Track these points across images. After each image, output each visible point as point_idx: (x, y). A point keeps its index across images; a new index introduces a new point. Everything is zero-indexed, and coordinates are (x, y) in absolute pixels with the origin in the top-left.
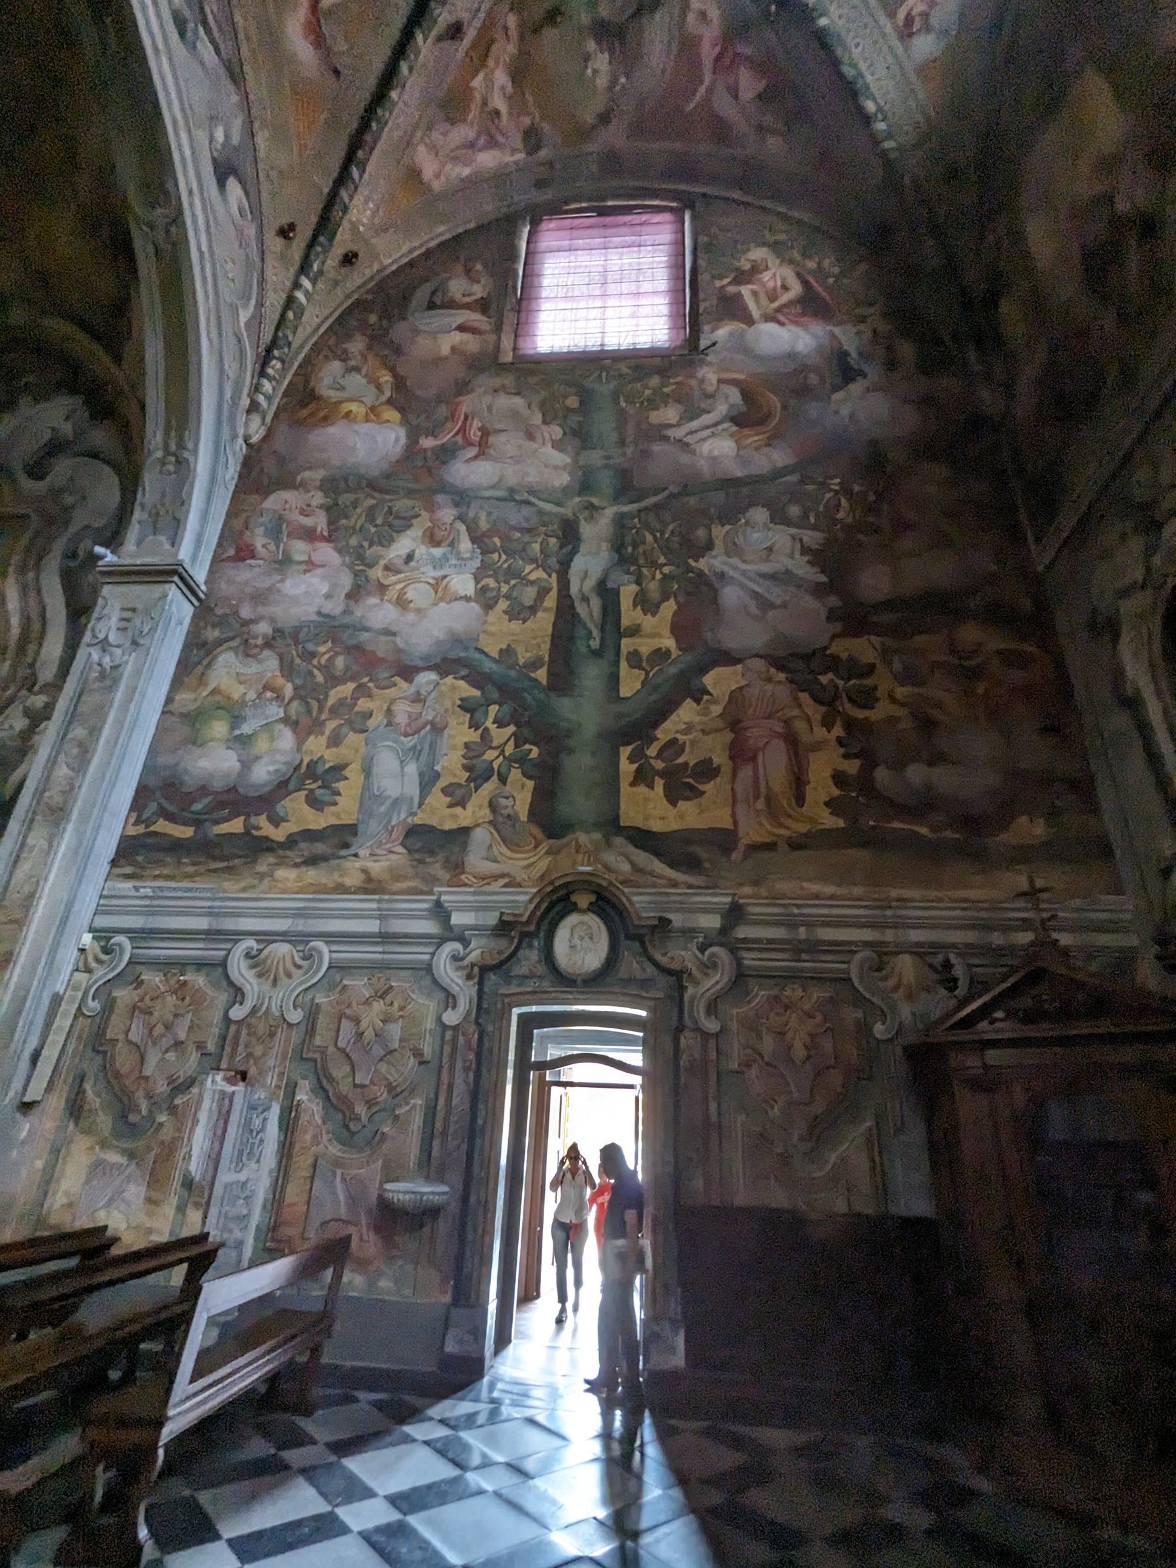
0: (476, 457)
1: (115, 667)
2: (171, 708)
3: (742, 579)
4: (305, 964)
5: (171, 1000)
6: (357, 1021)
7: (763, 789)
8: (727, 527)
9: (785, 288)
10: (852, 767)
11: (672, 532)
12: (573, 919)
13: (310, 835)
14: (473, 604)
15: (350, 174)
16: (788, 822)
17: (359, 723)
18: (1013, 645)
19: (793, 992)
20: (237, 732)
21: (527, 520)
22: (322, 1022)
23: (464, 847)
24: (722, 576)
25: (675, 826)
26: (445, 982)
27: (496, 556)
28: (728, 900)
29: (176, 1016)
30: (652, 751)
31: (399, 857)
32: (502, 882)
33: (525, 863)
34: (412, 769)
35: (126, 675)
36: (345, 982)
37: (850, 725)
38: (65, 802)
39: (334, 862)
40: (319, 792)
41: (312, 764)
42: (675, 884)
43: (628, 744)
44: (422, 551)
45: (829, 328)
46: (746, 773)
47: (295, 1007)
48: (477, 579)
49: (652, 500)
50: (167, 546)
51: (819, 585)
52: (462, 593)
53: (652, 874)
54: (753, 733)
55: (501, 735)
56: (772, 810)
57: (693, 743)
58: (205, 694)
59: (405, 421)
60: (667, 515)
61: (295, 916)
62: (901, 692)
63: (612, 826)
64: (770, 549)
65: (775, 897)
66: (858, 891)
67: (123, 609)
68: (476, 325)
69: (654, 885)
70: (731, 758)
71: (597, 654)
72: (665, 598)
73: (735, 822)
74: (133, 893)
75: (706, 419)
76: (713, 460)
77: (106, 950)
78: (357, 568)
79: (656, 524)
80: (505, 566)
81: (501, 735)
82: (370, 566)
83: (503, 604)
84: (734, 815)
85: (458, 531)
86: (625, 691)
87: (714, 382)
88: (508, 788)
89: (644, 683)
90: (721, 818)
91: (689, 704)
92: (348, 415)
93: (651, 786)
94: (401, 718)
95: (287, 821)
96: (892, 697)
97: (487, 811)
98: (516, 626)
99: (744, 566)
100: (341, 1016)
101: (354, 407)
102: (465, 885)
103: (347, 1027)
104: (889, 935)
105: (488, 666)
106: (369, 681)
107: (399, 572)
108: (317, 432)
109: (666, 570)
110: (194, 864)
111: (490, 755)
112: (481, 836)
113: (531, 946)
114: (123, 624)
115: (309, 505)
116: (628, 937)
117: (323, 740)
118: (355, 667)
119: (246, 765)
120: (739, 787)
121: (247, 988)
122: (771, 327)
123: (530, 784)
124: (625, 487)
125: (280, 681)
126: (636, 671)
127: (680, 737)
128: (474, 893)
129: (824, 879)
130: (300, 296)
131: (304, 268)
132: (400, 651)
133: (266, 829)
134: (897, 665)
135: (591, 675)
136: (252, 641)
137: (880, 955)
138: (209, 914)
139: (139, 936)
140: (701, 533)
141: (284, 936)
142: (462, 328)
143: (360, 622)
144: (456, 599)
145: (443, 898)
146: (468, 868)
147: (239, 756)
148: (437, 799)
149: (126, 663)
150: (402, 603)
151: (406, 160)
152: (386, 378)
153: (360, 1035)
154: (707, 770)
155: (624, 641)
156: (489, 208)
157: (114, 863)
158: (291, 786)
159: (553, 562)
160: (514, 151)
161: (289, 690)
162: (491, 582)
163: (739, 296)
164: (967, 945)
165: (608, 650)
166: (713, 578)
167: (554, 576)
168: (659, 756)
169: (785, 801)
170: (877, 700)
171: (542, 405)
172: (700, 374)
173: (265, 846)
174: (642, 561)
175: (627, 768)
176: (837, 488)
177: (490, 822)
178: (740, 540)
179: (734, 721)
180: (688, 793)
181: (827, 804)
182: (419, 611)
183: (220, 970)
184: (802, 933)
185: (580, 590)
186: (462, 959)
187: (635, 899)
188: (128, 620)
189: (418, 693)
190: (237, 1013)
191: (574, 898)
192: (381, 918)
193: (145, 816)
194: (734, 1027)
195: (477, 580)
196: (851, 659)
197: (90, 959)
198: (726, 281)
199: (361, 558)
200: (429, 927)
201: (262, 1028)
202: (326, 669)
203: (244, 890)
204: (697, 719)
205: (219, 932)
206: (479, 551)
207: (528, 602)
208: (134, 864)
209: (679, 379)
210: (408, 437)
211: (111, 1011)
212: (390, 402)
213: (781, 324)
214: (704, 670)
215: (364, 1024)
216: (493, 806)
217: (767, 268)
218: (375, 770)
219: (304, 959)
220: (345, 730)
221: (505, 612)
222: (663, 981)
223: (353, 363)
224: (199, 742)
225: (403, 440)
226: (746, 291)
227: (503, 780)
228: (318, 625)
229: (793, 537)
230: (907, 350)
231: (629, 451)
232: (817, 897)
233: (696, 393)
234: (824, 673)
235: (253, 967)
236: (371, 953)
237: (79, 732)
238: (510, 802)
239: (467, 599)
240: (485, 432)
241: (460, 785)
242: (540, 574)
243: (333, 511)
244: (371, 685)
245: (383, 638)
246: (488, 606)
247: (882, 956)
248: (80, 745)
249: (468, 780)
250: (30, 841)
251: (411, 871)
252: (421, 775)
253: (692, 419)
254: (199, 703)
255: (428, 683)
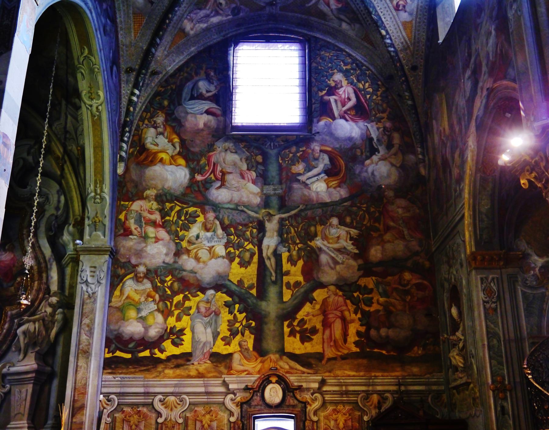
0: (220, 187)
1: (93, 293)
2: (111, 304)
3: (327, 251)
4: (181, 403)
5: (136, 417)
6: (202, 422)
7: (333, 338)
8: (323, 226)
9: (349, 99)
10: (363, 329)
11: (301, 229)
12: (270, 386)
13: (174, 357)
14: (225, 260)
15: (156, 41)
16: (341, 350)
17: (187, 311)
18: (420, 281)
19: (340, 407)
20: (140, 315)
21: (244, 220)
22: (190, 422)
23: (231, 360)
24: (320, 249)
25: (303, 351)
26: (229, 408)
27: (232, 237)
28: (321, 378)
29: (139, 422)
30: (295, 323)
31: (207, 365)
32: (246, 373)
33: (253, 366)
34: (209, 330)
35: (99, 296)
36: (196, 409)
37: (363, 313)
38: (88, 349)
39: (186, 367)
40: (176, 340)
41: (171, 328)
42: (304, 373)
43: (286, 321)
44: (203, 234)
45: (366, 124)
46: (327, 332)
47: (180, 418)
48: (226, 246)
49: (293, 212)
50: (102, 237)
51: (355, 254)
52: (221, 254)
53: (296, 369)
54: (331, 316)
55: (241, 317)
56: (336, 345)
57: (310, 320)
58: (124, 298)
59: (187, 166)
60: (300, 220)
61: (175, 387)
62: (382, 300)
63: (282, 352)
64: (338, 237)
65: (336, 376)
66: (362, 374)
67: (91, 267)
68: (214, 110)
69: (296, 373)
70: (323, 326)
71: (275, 283)
72: (299, 259)
73: (324, 350)
74: (114, 380)
75: (315, 171)
76: (317, 193)
77: (109, 400)
78: (177, 241)
79: (294, 224)
80: (237, 242)
81: (241, 317)
82: (182, 240)
83: (237, 260)
84: (323, 347)
85: (216, 224)
86: (285, 299)
87: (318, 151)
88: (244, 338)
89: (292, 296)
90: (318, 349)
91: (308, 304)
92: (161, 160)
93: (295, 337)
94: (203, 310)
95: (166, 351)
96: (378, 303)
97: (238, 347)
98: (243, 269)
99: (328, 245)
100: (196, 420)
101: (163, 155)
102: (233, 374)
103: (198, 424)
104: (371, 388)
105: (234, 288)
106: (189, 294)
107: (194, 244)
108: (150, 168)
109: (300, 246)
110: (134, 368)
111: (237, 325)
112: (237, 356)
113: (257, 395)
114: (92, 274)
115: (151, 209)
116: (288, 392)
117: (174, 319)
118: (181, 288)
119: (147, 328)
120: (325, 337)
121: (162, 412)
122: (342, 122)
123: (253, 336)
124: (283, 206)
125: (153, 293)
126: (289, 291)
127: (306, 318)
128: (236, 377)
129: (351, 370)
130: (135, 99)
131: (136, 85)
132: (198, 280)
133: (158, 355)
134: (381, 290)
135: (272, 291)
136: (138, 275)
137: (367, 394)
138: (144, 387)
139: (119, 394)
140: (312, 229)
141: (172, 394)
142: (208, 112)
143: (181, 267)
144: (219, 257)
145: (226, 379)
146: (233, 368)
147: (143, 325)
148: (219, 342)
149: (97, 291)
150: (197, 259)
151: (179, 26)
152: (176, 140)
153: (203, 426)
154: (314, 331)
155: (284, 277)
156: (216, 38)
157: (104, 368)
158: (165, 338)
159: (255, 240)
160: (227, 16)
161: (157, 297)
162: (233, 251)
163: (329, 102)
164: (393, 391)
165: (278, 282)
166: (317, 250)
167: (256, 247)
168: (298, 325)
169: (340, 342)
170: (373, 303)
171: (247, 159)
172: (312, 147)
173: (159, 361)
174: (290, 242)
175: (287, 330)
176: (364, 209)
177: (239, 351)
178: (327, 232)
179: (324, 311)
180: (308, 339)
181: (354, 343)
182: (204, 262)
183: (151, 406)
184: (344, 388)
185: (267, 254)
186: (235, 400)
187: (291, 378)
188: (94, 272)
189: (208, 300)
190: (160, 420)
191: (271, 379)
192: (205, 386)
193: (111, 349)
194: (322, 418)
195: (226, 249)
196: (365, 286)
197: (103, 403)
198: (324, 92)
199: (177, 236)
200: (222, 389)
201: (169, 425)
202: (170, 288)
203: (154, 377)
204: (310, 310)
205: (148, 393)
206: (225, 234)
207: (247, 260)
208: (111, 368)
209: (304, 148)
210: (190, 174)
211: (115, 421)
212: (179, 154)
213: (347, 120)
214: (313, 290)
215: (204, 422)
216: (240, 345)
217: (342, 87)
218: (195, 331)
219: (181, 401)
220: (182, 314)
221: (238, 264)
222: (300, 405)
223: (160, 130)
224: (126, 318)
225: (188, 176)
226: (332, 99)
227: (243, 335)
228: (165, 268)
229: (347, 231)
230: (397, 138)
231: (284, 186)
232: (349, 376)
233: (311, 156)
234: (355, 292)
235: (163, 405)
236: (204, 399)
237: (86, 321)
238: (245, 343)
239: (223, 257)
240: (224, 174)
241: (226, 337)
242: (250, 246)
243: (164, 213)
244: (189, 295)
245: (191, 275)
246: (232, 260)
247: (368, 395)
248: (88, 326)
249: (230, 335)
250: (80, 364)
251: (213, 370)
252: (213, 333)
253: (310, 170)
254: (122, 302)
255: (212, 295)
